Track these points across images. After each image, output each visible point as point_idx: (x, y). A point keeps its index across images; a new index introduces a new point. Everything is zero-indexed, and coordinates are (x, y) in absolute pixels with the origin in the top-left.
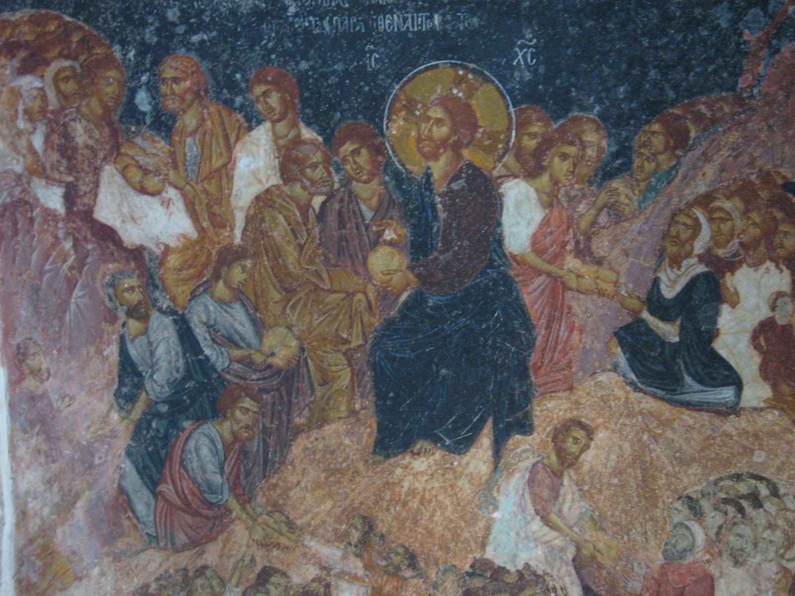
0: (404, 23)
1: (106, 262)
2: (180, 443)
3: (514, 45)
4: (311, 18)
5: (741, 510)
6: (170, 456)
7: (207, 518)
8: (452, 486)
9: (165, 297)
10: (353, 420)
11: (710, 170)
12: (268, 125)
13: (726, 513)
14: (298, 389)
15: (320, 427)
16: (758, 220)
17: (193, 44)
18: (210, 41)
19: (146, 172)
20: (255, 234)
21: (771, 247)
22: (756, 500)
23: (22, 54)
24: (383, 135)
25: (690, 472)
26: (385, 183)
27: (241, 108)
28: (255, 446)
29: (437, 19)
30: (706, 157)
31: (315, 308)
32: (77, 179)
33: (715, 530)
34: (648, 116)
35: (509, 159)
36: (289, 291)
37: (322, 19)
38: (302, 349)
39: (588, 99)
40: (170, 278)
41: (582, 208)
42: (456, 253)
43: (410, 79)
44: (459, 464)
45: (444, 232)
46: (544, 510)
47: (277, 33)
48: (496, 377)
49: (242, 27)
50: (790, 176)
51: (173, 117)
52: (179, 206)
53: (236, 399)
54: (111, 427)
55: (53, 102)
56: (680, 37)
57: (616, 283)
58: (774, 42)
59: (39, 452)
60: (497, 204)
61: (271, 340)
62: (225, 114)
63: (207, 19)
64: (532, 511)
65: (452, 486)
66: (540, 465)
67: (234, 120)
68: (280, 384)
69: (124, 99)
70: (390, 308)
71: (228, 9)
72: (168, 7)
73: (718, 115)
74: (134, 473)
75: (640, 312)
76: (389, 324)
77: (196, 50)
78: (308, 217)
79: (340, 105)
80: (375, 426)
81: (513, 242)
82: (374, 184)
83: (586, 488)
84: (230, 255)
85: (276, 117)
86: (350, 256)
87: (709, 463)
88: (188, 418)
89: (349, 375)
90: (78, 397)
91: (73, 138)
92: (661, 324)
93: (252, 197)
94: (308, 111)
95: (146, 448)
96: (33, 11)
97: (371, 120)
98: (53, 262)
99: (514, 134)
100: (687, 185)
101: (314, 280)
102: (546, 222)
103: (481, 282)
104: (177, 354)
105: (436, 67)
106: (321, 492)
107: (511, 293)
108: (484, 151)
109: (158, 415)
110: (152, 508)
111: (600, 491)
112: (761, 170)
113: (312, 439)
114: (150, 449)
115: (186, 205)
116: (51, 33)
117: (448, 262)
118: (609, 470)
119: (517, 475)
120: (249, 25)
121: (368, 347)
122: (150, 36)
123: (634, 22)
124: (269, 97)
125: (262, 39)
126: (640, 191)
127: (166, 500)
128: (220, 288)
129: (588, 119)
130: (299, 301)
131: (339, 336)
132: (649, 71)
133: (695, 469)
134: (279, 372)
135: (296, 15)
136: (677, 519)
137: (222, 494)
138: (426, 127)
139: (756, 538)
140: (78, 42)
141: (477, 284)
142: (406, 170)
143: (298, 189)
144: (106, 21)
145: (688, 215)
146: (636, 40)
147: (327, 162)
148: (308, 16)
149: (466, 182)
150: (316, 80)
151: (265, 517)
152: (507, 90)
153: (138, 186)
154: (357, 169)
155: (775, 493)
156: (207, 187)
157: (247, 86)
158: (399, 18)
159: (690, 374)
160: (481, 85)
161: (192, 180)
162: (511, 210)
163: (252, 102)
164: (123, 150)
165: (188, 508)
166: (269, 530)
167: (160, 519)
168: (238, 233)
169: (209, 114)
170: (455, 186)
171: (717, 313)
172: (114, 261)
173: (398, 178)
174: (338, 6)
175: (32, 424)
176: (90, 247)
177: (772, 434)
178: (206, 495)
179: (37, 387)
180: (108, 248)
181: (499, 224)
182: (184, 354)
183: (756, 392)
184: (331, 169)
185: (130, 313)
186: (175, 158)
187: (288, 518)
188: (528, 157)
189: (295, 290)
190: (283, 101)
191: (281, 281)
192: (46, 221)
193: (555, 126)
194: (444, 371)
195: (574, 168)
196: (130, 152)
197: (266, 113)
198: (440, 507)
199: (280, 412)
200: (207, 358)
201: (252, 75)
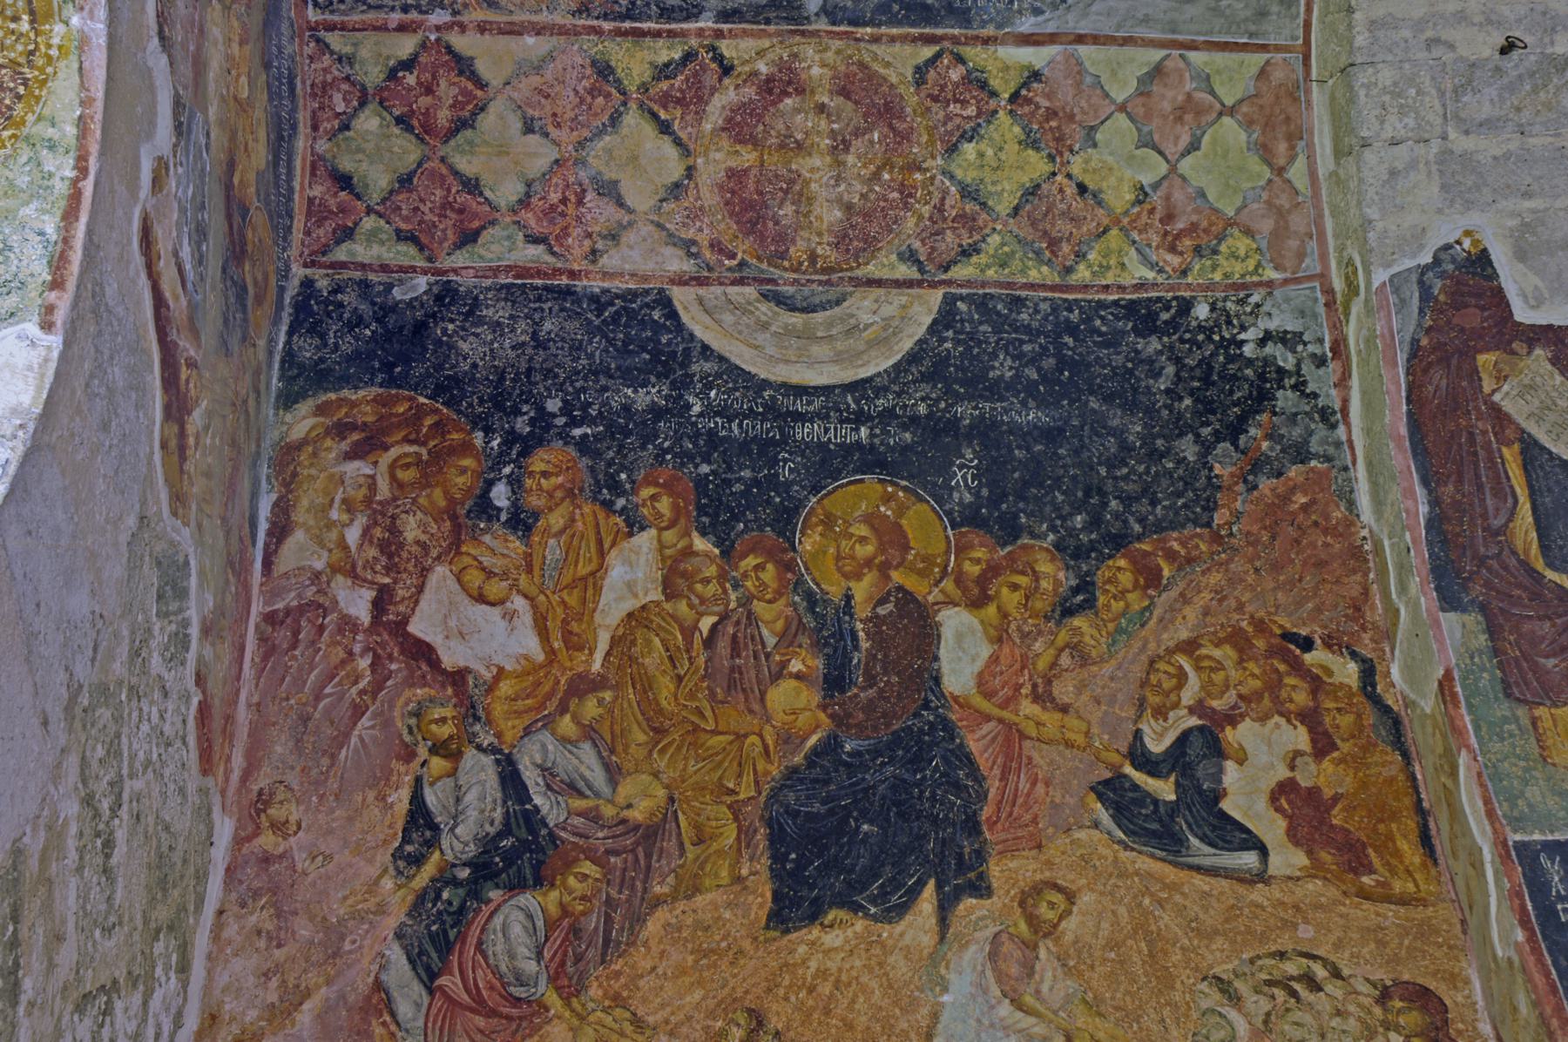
1: (413, 685)
2: (481, 919)
3: (952, 464)
5: (1293, 994)
6: (462, 937)
7: (509, 1018)
8: (881, 965)
10: (737, 888)
11: (1191, 613)
12: (653, 532)
13: (1273, 997)
14: (661, 849)
15: (688, 898)
16: (1257, 671)
19: (489, 574)
21: (1276, 700)
22: (1315, 986)
23: (356, 437)
24: (794, 549)
25: (1214, 947)
26: (795, 603)
28: (593, 922)
29: (864, 432)
30: (1184, 598)
31: (692, 752)
32: (395, 582)
33: (1261, 1018)
35: (948, 584)
36: (660, 731)
37: (730, 421)
38: (671, 800)
40: (498, 710)
41: (1038, 646)
42: (881, 691)
43: (830, 493)
44: (891, 936)
45: (867, 664)
46: (1015, 991)
47: (676, 432)
48: (937, 833)
49: (635, 423)
50: (1288, 625)
51: (536, 515)
52: (526, 617)
53: (569, 864)
54: (377, 900)
55: (384, 490)
56: (1142, 468)
57: (1087, 734)
58: (1250, 478)
59: (259, 933)
61: (626, 790)
62: (601, 516)
64: (999, 993)
65: (881, 965)
66: (1004, 937)
68: (637, 843)
69: (478, 492)
70: (793, 753)
72: (550, 396)
73: (1194, 553)
74: (404, 960)
75: (1122, 766)
76: (794, 770)
80: (769, 895)
83: (1072, 963)
84: (583, 686)
86: (744, 690)
87: (1239, 938)
88: (497, 886)
89: (734, 835)
90: (336, 857)
91: (401, 533)
92: (1150, 781)
93: (624, 614)
94: (705, 520)
95: (428, 927)
96: (381, 391)
97: (781, 533)
98: (340, 684)
100: (1165, 628)
101: (693, 718)
102: (994, 659)
104: (495, 801)
106: (687, 980)
107: (953, 739)
109: (455, 882)
110: (424, 1010)
111: (1092, 967)
112: (1252, 617)
113: (678, 912)
114: (434, 928)
115: (535, 620)
116: (398, 415)
117: (871, 700)
118: (1102, 942)
119: (973, 948)
120: (644, 423)
121: (762, 799)
122: (522, 425)
125: (656, 437)
127: (448, 998)
128: (566, 724)
129: (1041, 548)
130: (670, 744)
131: (723, 786)
133: (1219, 942)
134: (637, 827)
135: (701, 415)
136: (1205, 1004)
137: (536, 986)
139: (1321, 1027)
140: (430, 427)
141: (909, 727)
144: (470, 405)
145: (1169, 663)
146: (1092, 468)
147: (722, 577)
151: (599, 1013)
153: (475, 593)
155: (1336, 974)
156: (567, 598)
159: (1196, 836)
164: (464, 549)
165: (479, 1005)
166: (602, 1030)
167: (435, 1022)
170: (881, 611)
171: (1221, 771)
172: (424, 686)
174: (751, 409)
175: (256, 894)
176: (394, 667)
177: (1318, 907)
178: (512, 989)
179: (277, 845)
181: (936, 658)
182: (505, 802)
183: (1286, 859)
185: (433, 751)
187: (634, 1015)
188: (971, 584)
190: (675, 508)
191: (648, 720)
192: (340, 631)
194: (865, 827)
196: (473, 552)
198: (864, 992)
199: (633, 879)
200: (537, 809)
201: (640, 476)
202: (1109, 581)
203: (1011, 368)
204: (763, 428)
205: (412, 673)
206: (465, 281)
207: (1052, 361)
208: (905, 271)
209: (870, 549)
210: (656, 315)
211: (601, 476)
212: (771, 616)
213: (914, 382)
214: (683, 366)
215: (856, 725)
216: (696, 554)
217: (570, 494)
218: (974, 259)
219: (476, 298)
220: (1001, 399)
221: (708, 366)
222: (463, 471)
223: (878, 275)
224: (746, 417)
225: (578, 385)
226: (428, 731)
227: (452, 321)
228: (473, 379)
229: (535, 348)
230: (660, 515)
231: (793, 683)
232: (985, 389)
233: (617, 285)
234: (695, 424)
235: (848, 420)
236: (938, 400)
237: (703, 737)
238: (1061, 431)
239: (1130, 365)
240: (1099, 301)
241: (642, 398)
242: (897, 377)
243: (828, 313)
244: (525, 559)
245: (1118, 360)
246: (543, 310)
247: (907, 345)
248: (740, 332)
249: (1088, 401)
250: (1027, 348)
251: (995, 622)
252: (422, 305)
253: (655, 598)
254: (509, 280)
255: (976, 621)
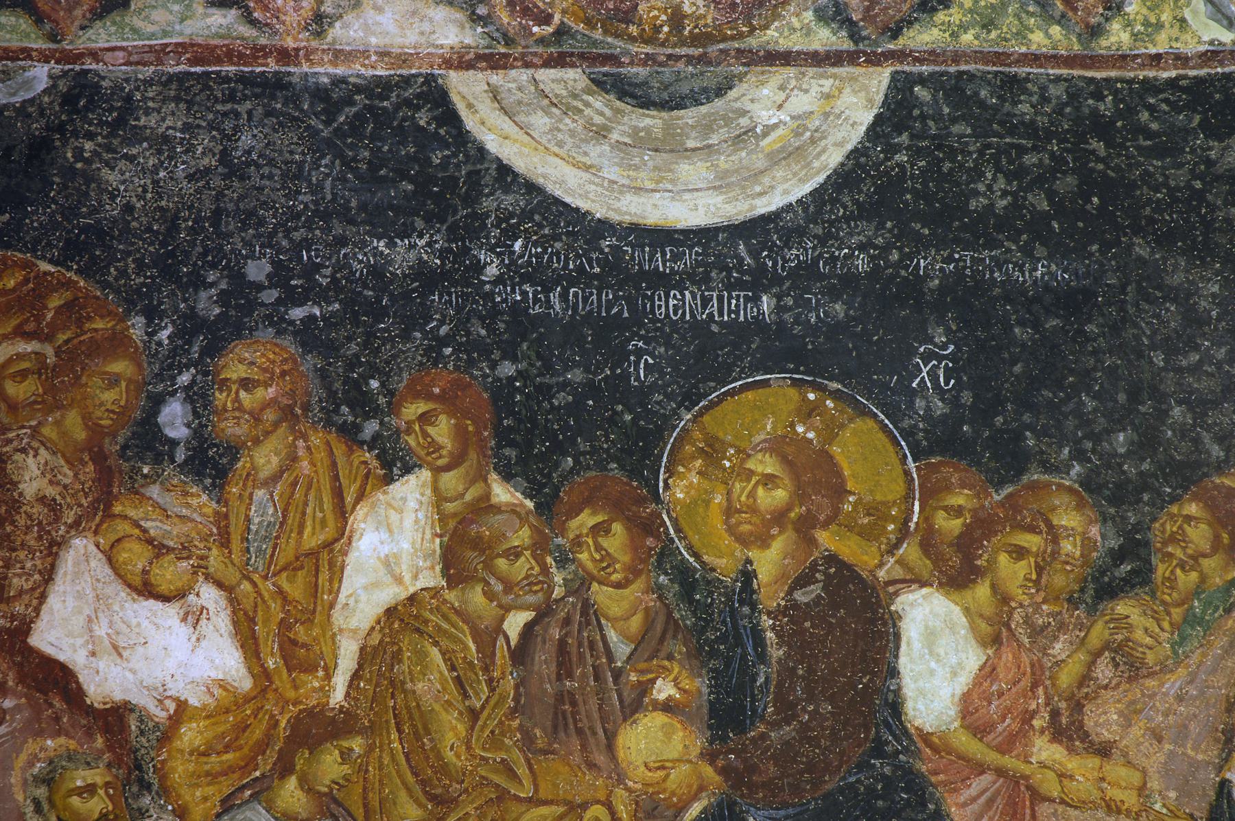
0: (704, 307)
1: (40, 733)
4: (527, 287)
9: (161, 807)
12: (426, 474)
17: (292, 323)
18: (323, 318)
19: (159, 549)
20: (377, 685)
24: (657, 498)
26: (660, 587)
27: (373, 443)
29: (766, 303)
34: (1174, 489)
35: (910, 550)
37: (547, 290)
39: (1059, 452)
40: (180, 770)
41: (1059, 648)
42: (805, 727)
43: (713, 405)
45: (780, 685)
47: (459, 310)
49: (391, 295)
51: (233, 451)
52: (220, 621)
57: (1142, 789)
60: (887, 633)
62: (339, 450)
63: (324, 282)
67: (356, 463)
69: (138, 414)
71: (368, 265)
77: (295, 334)
78: (494, 654)
79: (574, 443)
81: (921, 706)
82: (636, 590)
84: (318, 727)
85: (440, 462)
86: (580, 732)
91: (15, 484)
93: (381, 610)
97: (634, 473)
99: (917, 508)
102: (988, 672)
103: (858, 781)
105: (765, 384)
107: (924, 805)
108: (860, 534)
115: (235, 623)
120: (406, 295)
122: (207, 304)
123: (1136, 326)
124: (432, 424)
126: (1171, 624)
129: (1060, 486)
132: (1172, 408)
135: (499, 280)
138: (743, 489)
140: (58, 310)
141: (851, 786)
142: (703, 564)
143: (477, 597)
144: (123, 273)
146: (1140, 355)
147: (540, 546)
148: (520, 284)
149: (823, 588)
150: (528, 396)
152: (902, 431)
153: (137, 581)
154: (602, 560)
156: (286, 586)
157: (389, 403)
158: (694, 298)
160: (851, 420)
161: (256, 570)
162: (917, 645)
163: (398, 432)
164: (117, 509)
168: (340, 682)
169: (308, 448)
170: (801, 597)
172: (58, 733)
173: (687, 580)
174: (580, 269)
180: (51, 705)
181: (894, 673)
184: (549, 560)
186: (227, 526)
189: (455, 801)
190: (460, 433)
191: (423, 783)
193: (997, 498)
195: (1039, 575)
196: (132, 513)
197: (422, 453)
201: (401, 383)
202: (1172, 539)
203: (1005, 193)
204: (602, 301)
205: (37, 711)
206: (113, 69)
207: (1071, 180)
208: (825, 38)
209: (781, 495)
210: (423, 118)
211: (337, 385)
212: (622, 608)
213: (847, 219)
214: (470, 199)
215: (764, 785)
216: (497, 509)
217: (287, 414)
218: (941, 16)
219: (129, 99)
220: (991, 244)
221: (508, 201)
222: (113, 381)
223: (784, 44)
224: (573, 282)
225: (297, 236)
226: (67, 807)
227: (90, 136)
228: (126, 230)
229: (225, 177)
230: (436, 447)
231: (660, 718)
232: (964, 228)
233: (357, 70)
234: (491, 295)
235: (740, 285)
236: (886, 249)
237: (515, 809)
238: (1089, 294)
239: (1198, 185)
240: (1146, 81)
241: (404, 254)
242: (819, 211)
243: (703, 109)
244: (217, 523)
245: (1179, 177)
246: (237, 115)
247: (834, 158)
248: (560, 144)
249: (1130, 246)
250: (1030, 159)
251: (989, 611)
252: (42, 113)
253: (432, 584)
254: (182, 68)
255: (957, 610)
